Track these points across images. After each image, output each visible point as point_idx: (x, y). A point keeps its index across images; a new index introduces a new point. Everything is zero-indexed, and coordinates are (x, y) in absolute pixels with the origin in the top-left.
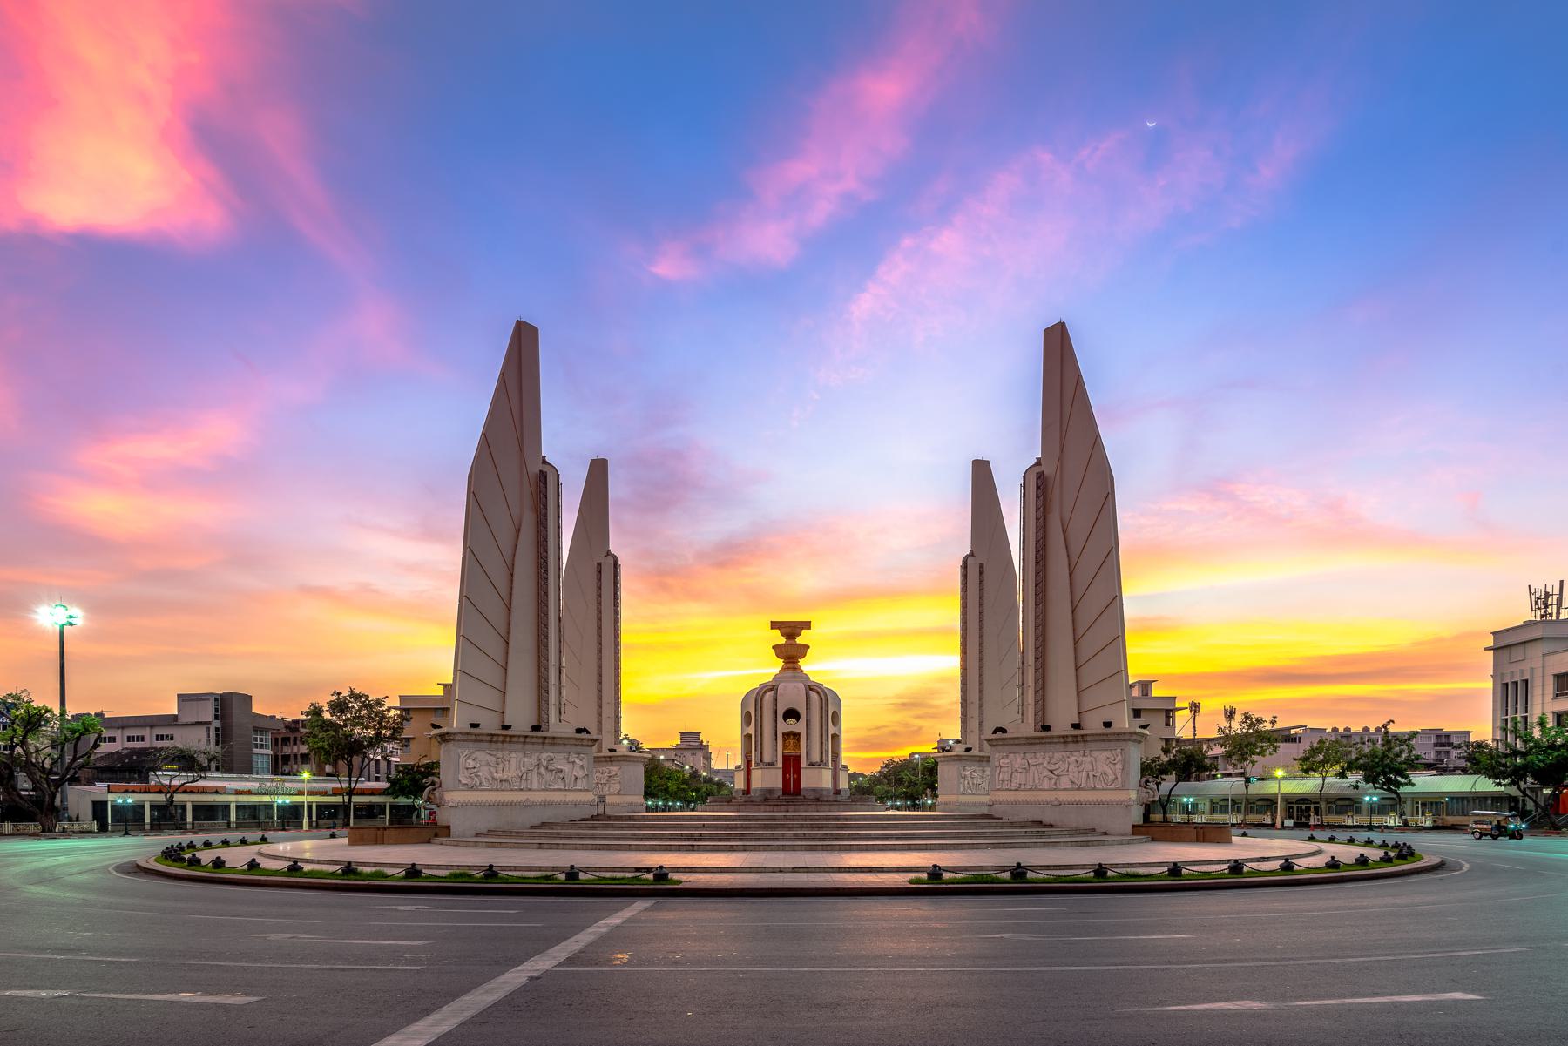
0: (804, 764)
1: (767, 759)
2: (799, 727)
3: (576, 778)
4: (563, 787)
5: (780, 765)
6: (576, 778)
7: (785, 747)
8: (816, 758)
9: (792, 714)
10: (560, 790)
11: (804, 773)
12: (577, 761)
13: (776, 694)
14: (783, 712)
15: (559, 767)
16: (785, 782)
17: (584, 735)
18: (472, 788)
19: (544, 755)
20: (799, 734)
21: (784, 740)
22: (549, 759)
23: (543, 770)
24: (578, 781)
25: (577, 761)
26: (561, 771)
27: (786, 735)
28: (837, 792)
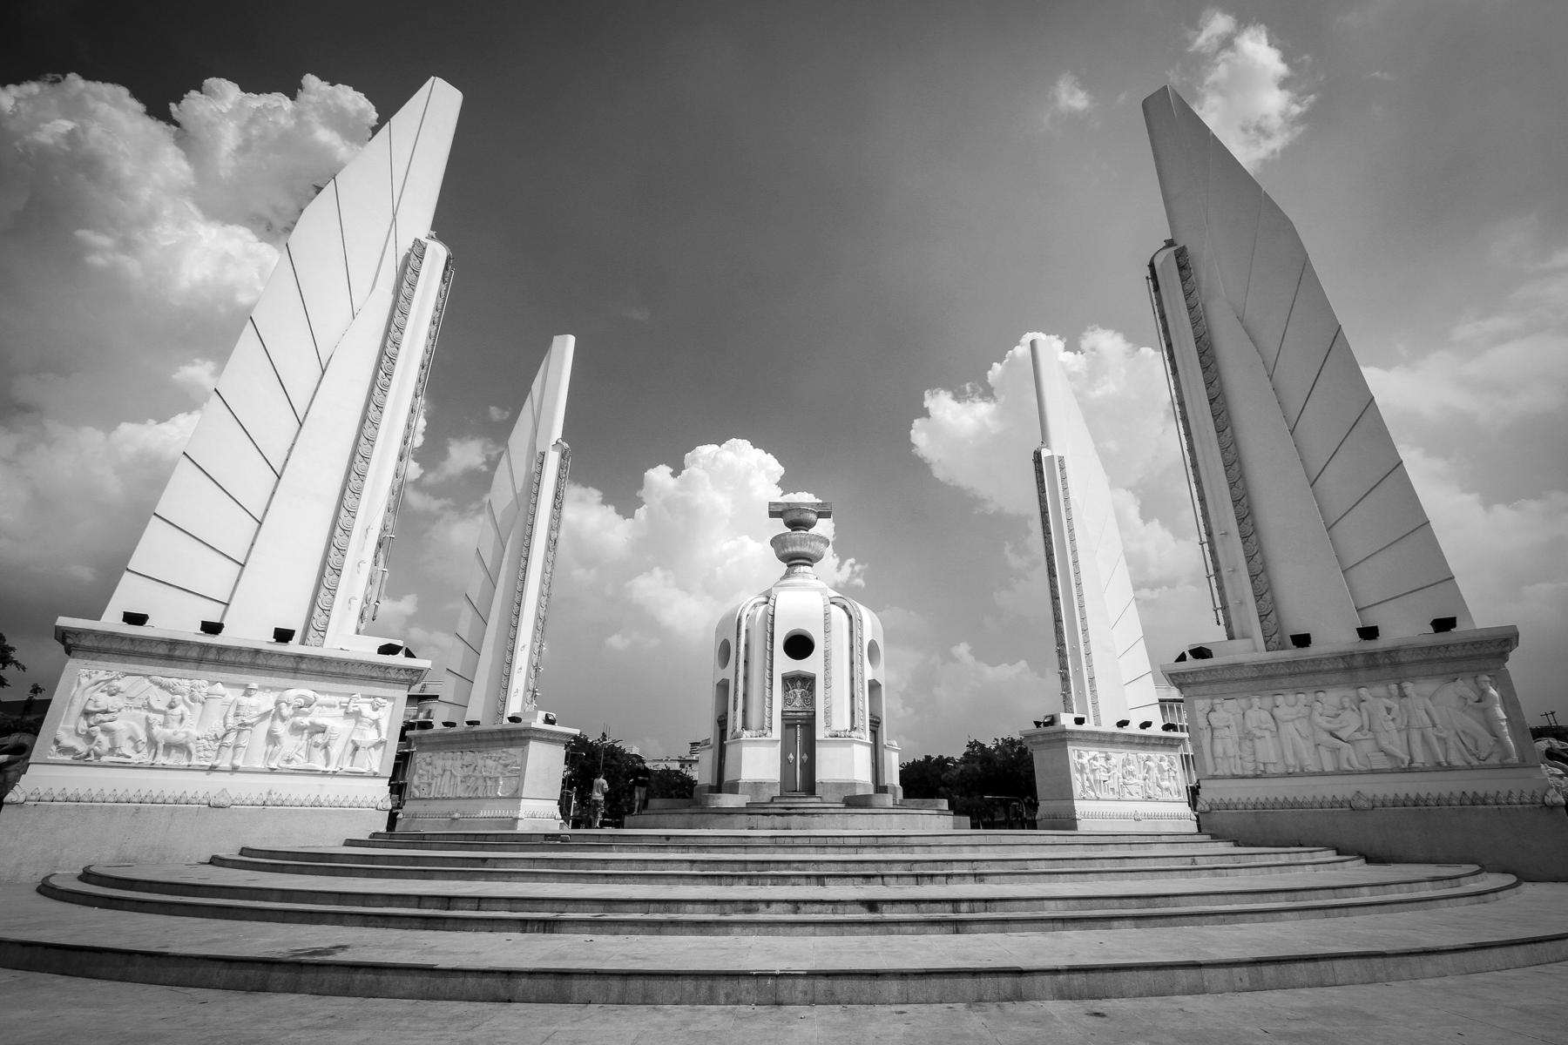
3: (356, 749)
5: (777, 733)
6: (356, 749)
7: (786, 701)
10: (312, 772)
11: (821, 753)
12: (366, 709)
15: (320, 721)
16: (786, 766)
17: (399, 659)
18: (83, 760)
19: (291, 694)
21: (786, 689)
24: (361, 751)
25: (366, 709)
26: (323, 730)
27: (790, 680)
28: (881, 789)
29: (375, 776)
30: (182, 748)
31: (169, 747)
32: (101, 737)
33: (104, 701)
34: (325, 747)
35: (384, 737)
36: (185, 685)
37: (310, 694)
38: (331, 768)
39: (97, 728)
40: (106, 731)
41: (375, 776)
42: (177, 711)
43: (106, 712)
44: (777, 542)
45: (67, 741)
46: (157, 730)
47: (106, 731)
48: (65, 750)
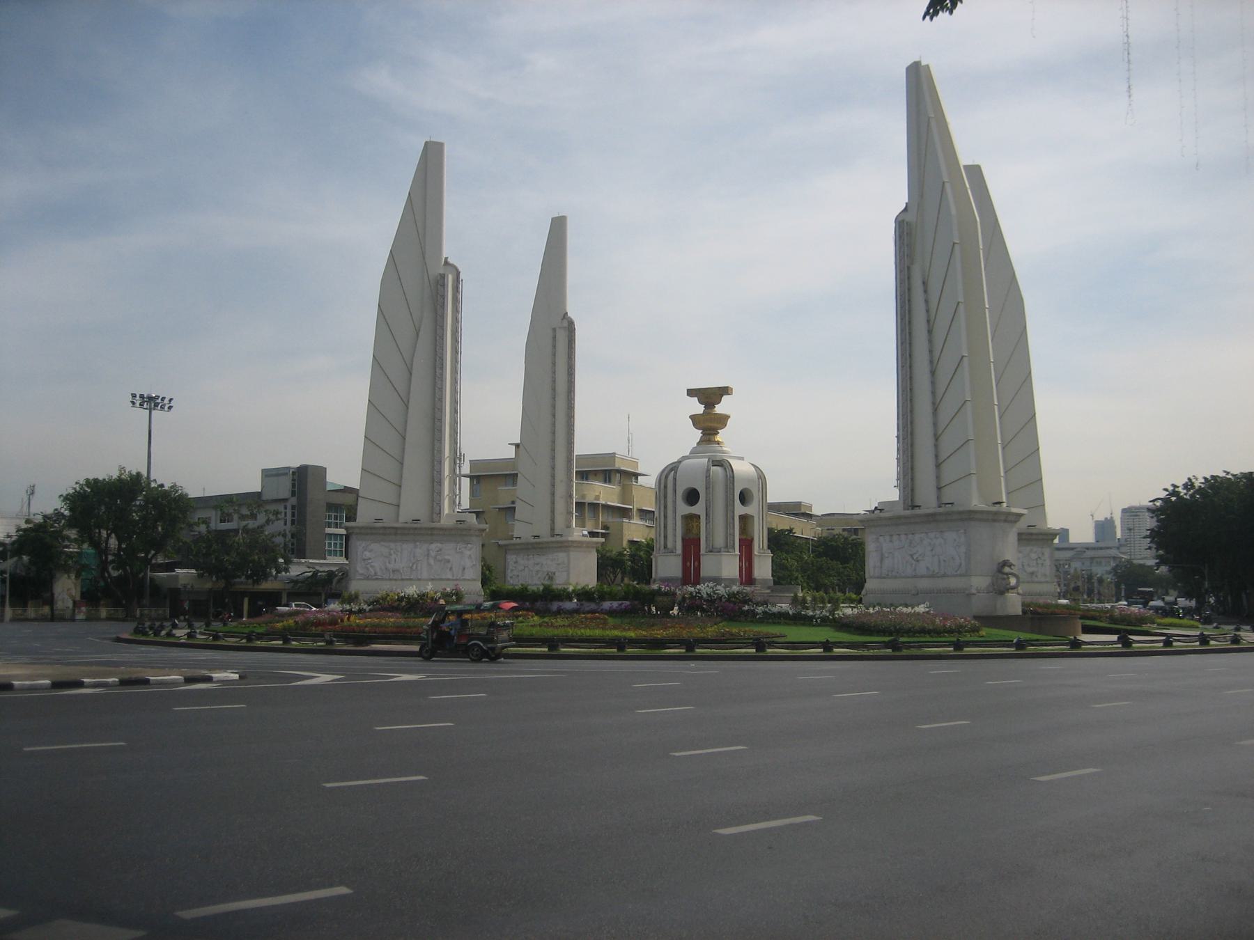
0: (703, 551)
1: (670, 545)
2: (699, 509)
3: (464, 569)
4: (451, 577)
8: (719, 540)
9: (692, 496)
13: (676, 473)
14: (681, 494)
15: (447, 557)
16: (686, 570)
19: (433, 546)
20: (698, 517)
22: (437, 549)
23: (432, 561)
26: (448, 561)
29: (474, 580)
30: (398, 571)
31: (393, 571)
32: (370, 569)
33: (367, 554)
34: (451, 569)
35: (474, 563)
36: (392, 545)
37: (439, 545)
38: (455, 578)
39: (368, 566)
40: (372, 566)
41: (474, 580)
42: (394, 556)
43: (370, 559)
44: (695, 419)
45: (361, 572)
46: (388, 564)
47: (372, 566)
48: (362, 574)
